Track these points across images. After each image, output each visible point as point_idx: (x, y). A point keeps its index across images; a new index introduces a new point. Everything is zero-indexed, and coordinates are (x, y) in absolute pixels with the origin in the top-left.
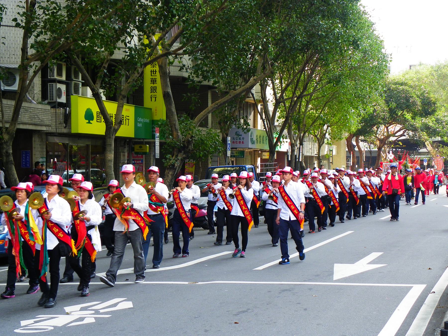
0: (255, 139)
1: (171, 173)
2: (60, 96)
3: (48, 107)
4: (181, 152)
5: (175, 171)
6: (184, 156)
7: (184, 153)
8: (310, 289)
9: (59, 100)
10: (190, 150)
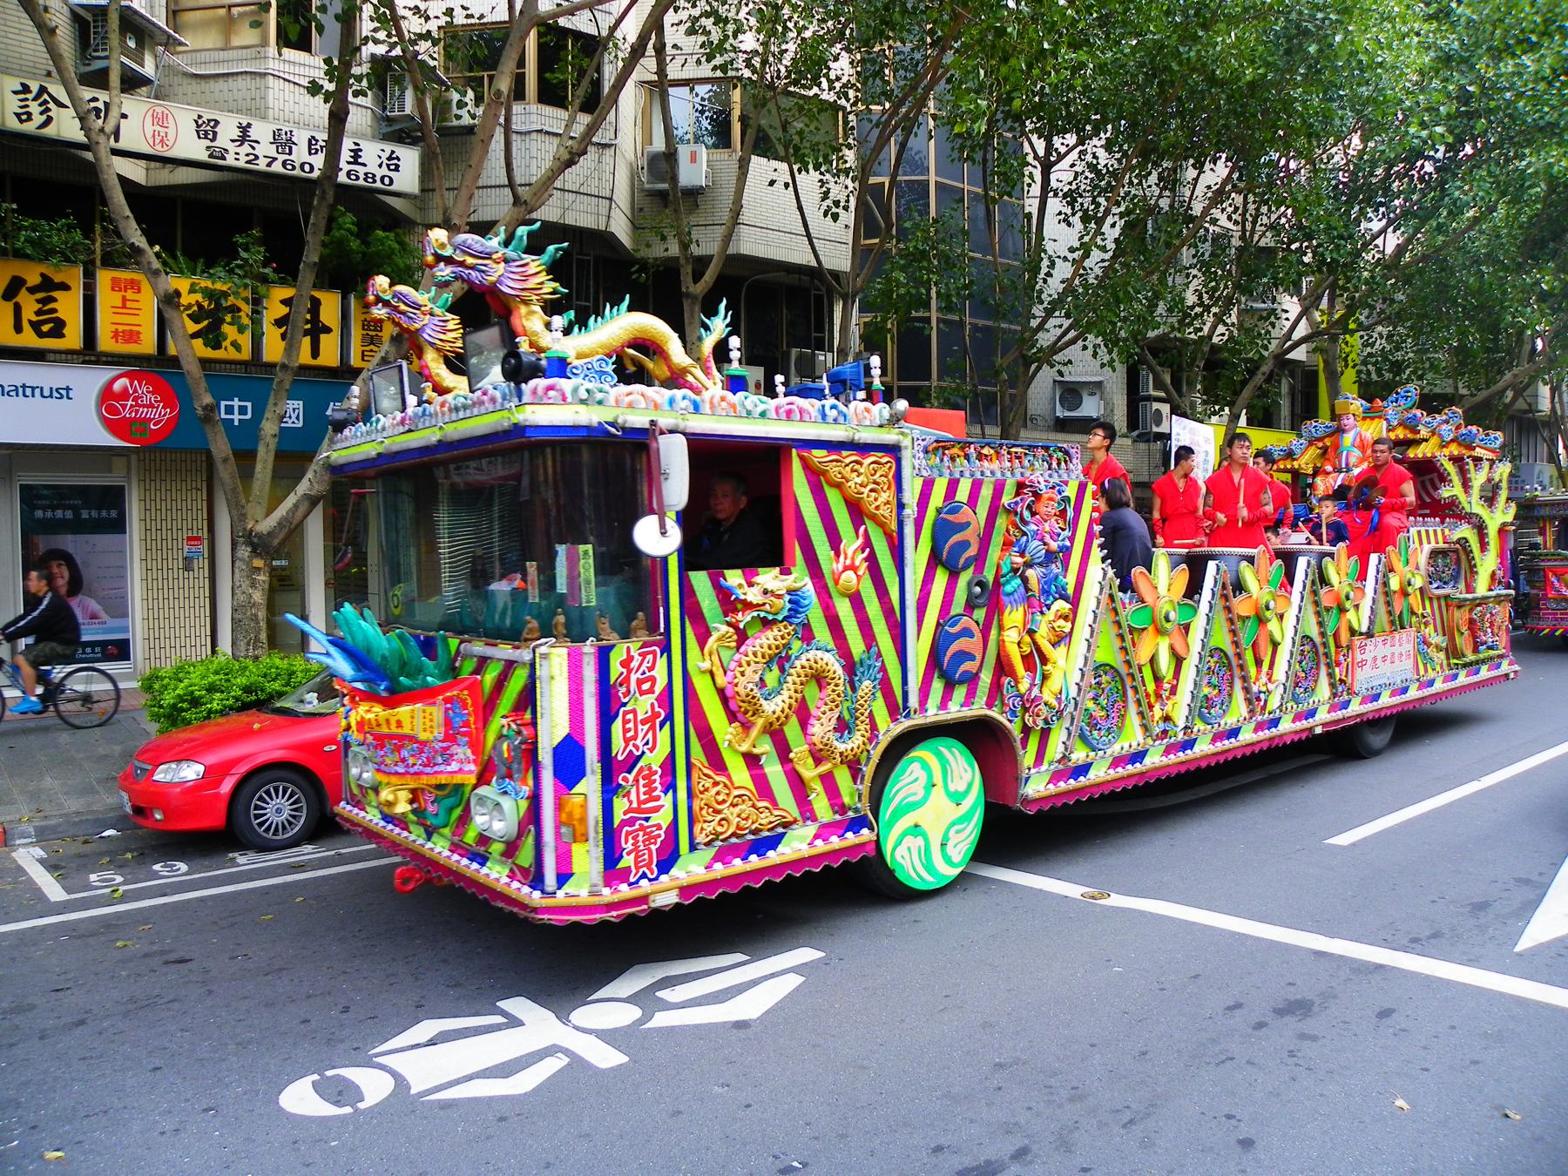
0: (1546, 482)
2: (1158, 423)
3: (1128, 442)
8: (1385, 1014)
9: (1155, 429)
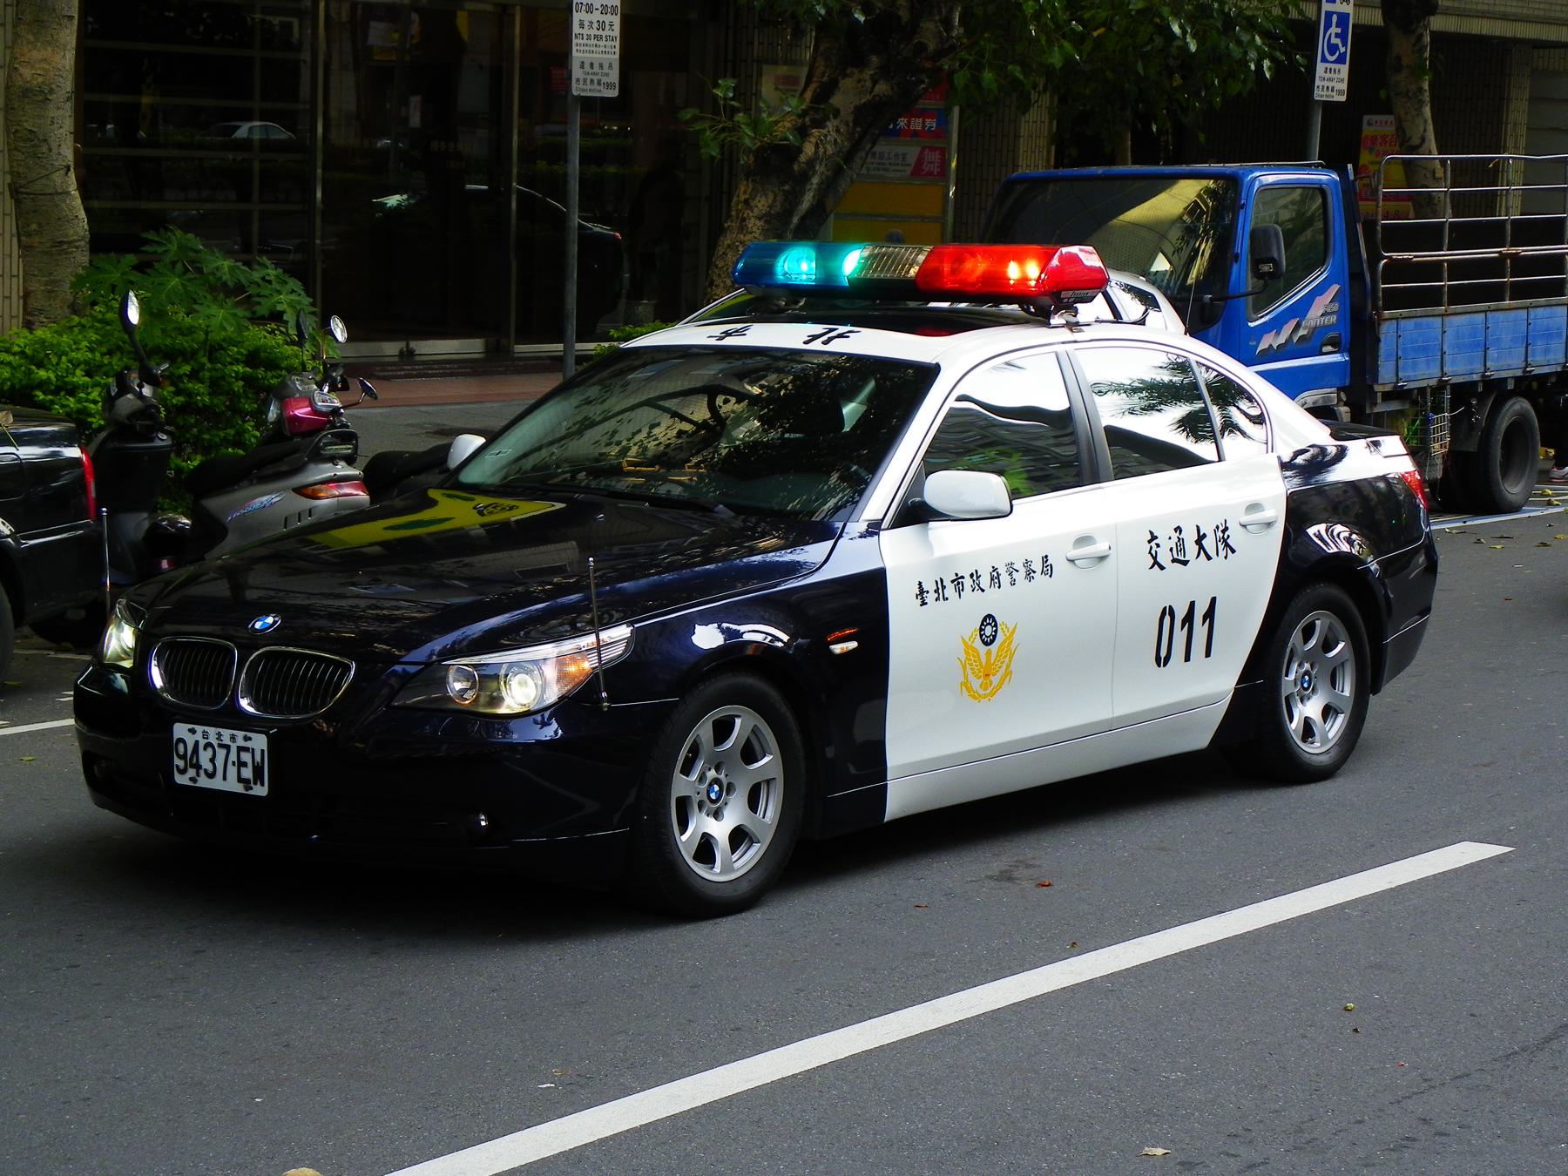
1: (761, 204)
4: (861, 63)
5: (793, 198)
6: (882, 88)
7: (884, 72)
10: (922, 47)
